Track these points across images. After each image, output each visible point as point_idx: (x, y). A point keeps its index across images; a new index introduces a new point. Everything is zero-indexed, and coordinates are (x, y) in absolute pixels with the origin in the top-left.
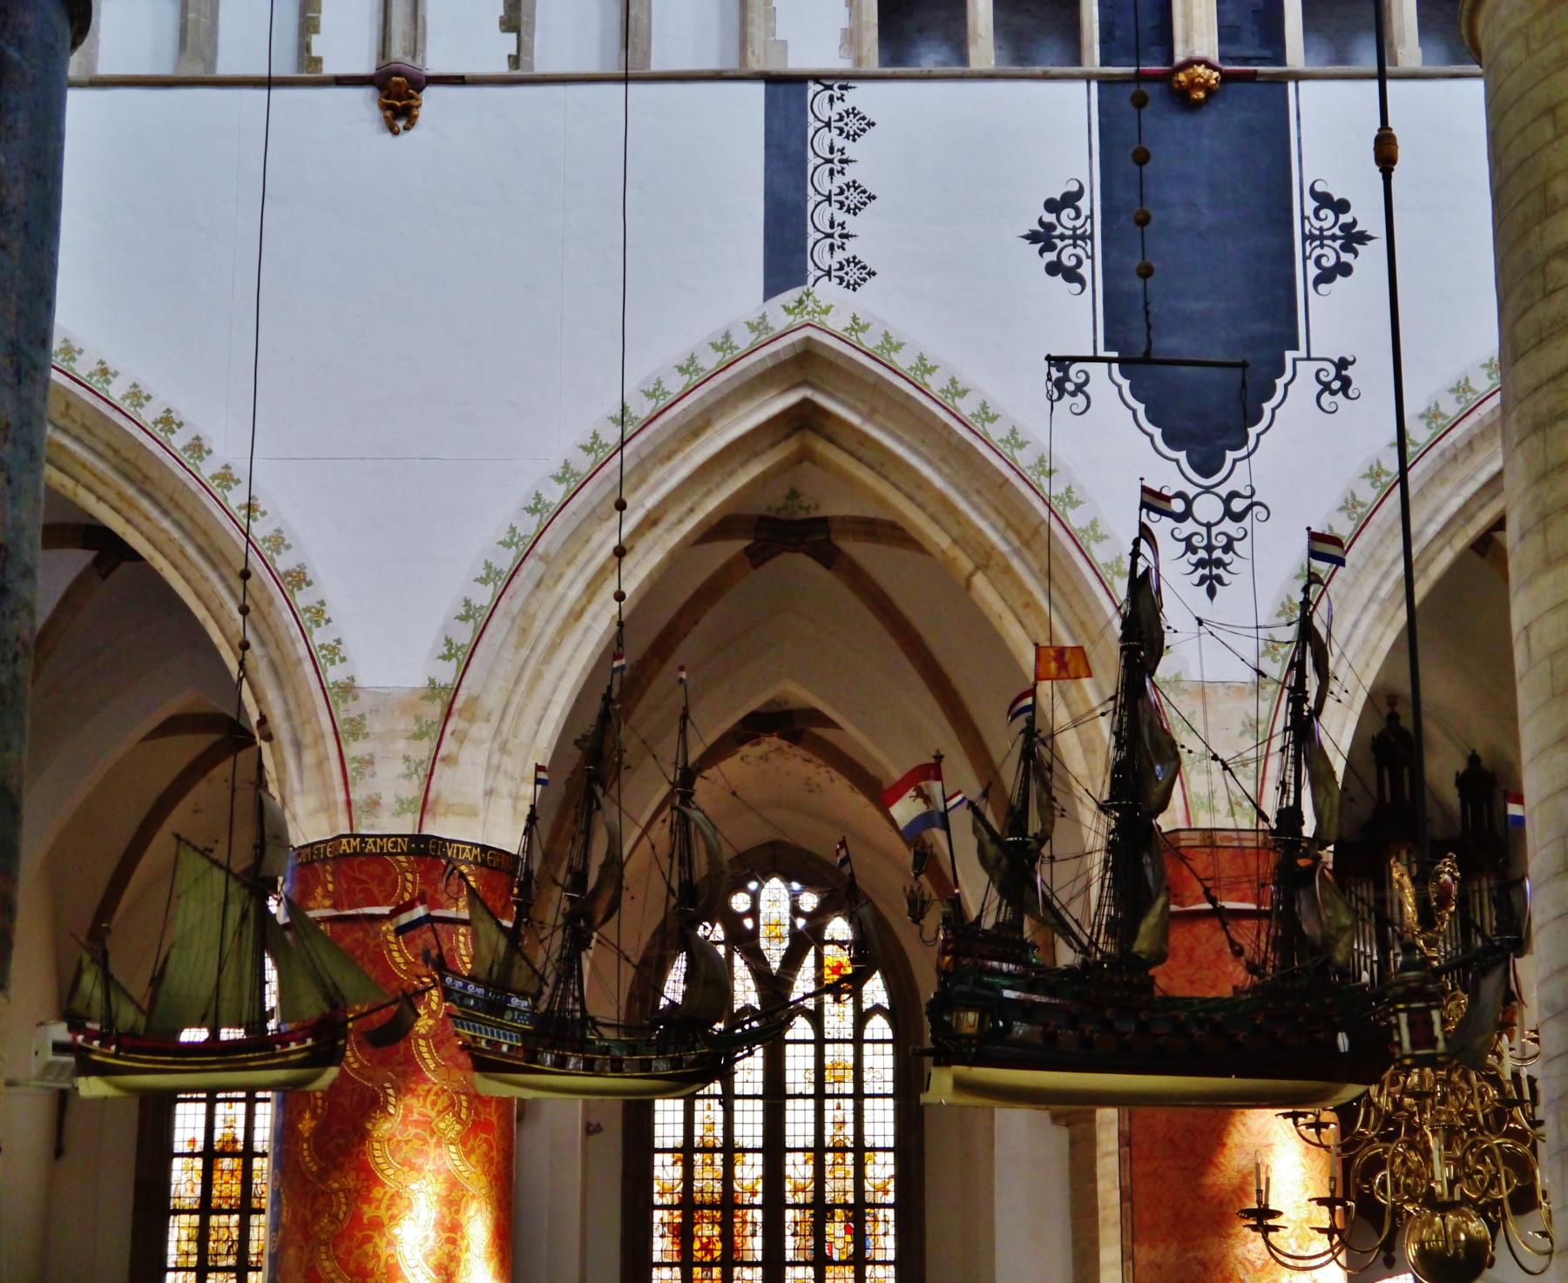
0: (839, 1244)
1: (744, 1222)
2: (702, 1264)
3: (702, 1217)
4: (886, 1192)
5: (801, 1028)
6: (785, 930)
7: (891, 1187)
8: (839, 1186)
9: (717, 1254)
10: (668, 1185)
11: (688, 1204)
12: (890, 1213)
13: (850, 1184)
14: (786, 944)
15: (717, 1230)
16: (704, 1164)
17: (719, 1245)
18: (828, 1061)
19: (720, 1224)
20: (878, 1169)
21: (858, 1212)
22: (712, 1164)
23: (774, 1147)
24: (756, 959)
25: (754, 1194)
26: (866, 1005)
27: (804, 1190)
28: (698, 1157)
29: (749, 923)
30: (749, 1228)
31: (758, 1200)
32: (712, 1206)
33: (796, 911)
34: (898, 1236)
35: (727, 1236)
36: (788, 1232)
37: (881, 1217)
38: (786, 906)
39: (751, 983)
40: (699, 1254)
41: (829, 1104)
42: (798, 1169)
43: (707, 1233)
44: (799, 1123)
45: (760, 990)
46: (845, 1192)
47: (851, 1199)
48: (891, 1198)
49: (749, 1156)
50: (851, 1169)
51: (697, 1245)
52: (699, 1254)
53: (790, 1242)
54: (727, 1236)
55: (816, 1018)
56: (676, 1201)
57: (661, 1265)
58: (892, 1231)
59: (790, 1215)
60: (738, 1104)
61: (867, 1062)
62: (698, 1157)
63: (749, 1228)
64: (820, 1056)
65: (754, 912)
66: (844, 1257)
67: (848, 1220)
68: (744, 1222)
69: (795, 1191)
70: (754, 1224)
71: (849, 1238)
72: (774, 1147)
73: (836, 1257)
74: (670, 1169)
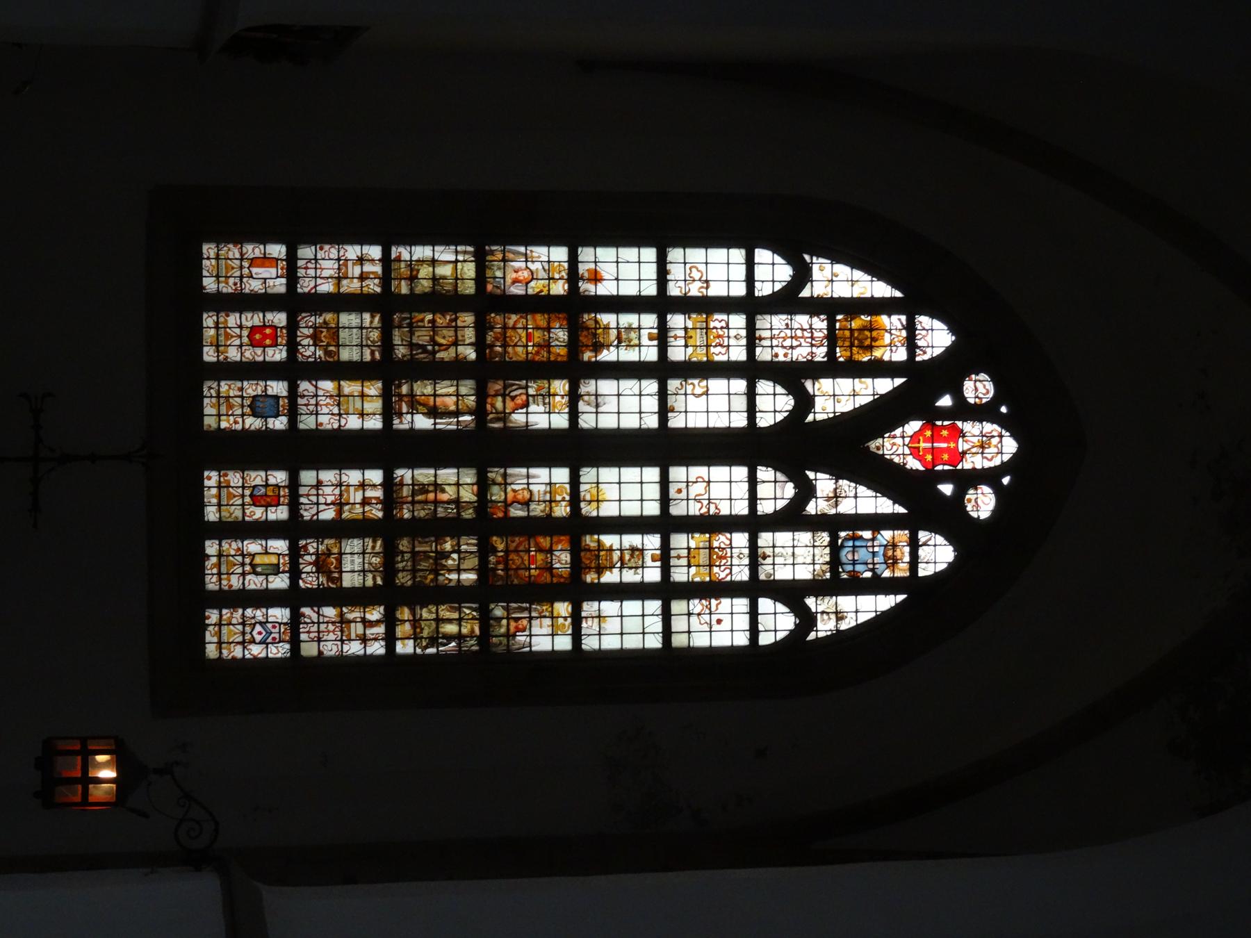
5: (775, 492)
23: (583, 448)
24: (882, 415)
29: (946, 401)
38: (974, 462)
39: (846, 406)
45: (840, 421)
72: (583, 448)
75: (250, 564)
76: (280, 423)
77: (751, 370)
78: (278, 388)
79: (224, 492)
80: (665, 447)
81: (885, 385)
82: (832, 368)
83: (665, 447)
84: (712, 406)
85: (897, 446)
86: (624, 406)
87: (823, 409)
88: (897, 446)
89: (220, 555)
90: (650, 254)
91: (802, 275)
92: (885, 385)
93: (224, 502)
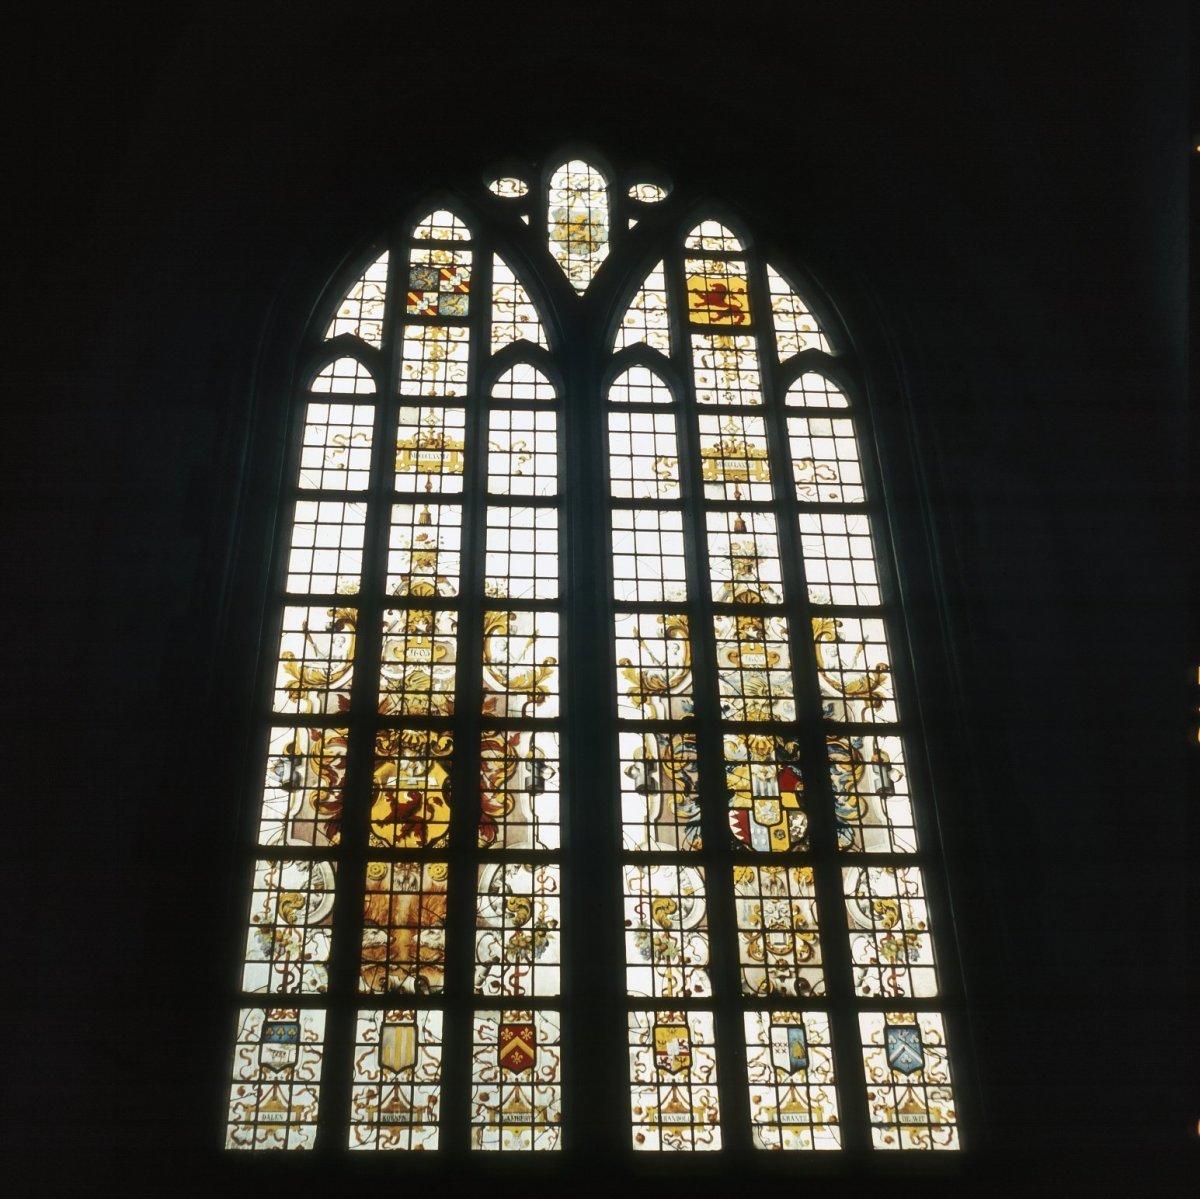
0: (766, 811)
1: (511, 761)
2: (392, 855)
3: (399, 745)
4: (877, 701)
6: (603, 233)
7: (886, 688)
8: (755, 672)
9: (435, 831)
10: (315, 671)
11: (364, 719)
12: (893, 747)
13: (782, 682)
14: (604, 252)
15: (438, 777)
16: (408, 632)
17: (443, 812)
18: (707, 444)
19: (445, 762)
20: (848, 653)
21: (811, 745)
22: (432, 630)
23: (587, 603)
24: (543, 280)
25: (537, 696)
26: (786, 351)
27: (665, 692)
28: (394, 619)
30: (524, 773)
31: (550, 708)
32: (427, 722)
33: (621, 206)
34: (917, 795)
35: (465, 791)
36: (626, 783)
37: (868, 753)
40: (388, 832)
41: (714, 520)
42: (645, 649)
43: (409, 780)
44: (646, 558)
46: (772, 700)
47: (786, 711)
48: (889, 713)
49: (523, 621)
50: (784, 651)
51: (381, 809)
52: (388, 832)
53: (633, 807)
54: (465, 791)
55: (676, 369)
56: (334, 706)
57: (279, 855)
58: (902, 786)
59: (629, 745)
60: (495, 515)
61: (798, 449)
62: (394, 619)
63: (524, 773)
64: (688, 437)
65: (536, 202)
66: (782, 846)
67: (783, 758)
68: (511, 761)
69: (644, 694)
70: (539, 764)
71: (790, 800)
72: (587, 603)
73: (760, 841)
74: (322, 642)
75: (791, 1074)
76: (549, 1024)
77: (478, 404)
78: (485, 1025)
79: (668, 1118)
80: (585, 503)
81: (502, 272)
82: (479, 320)
83: (585, 503)
84: (527, 448)
85: (582, 271)
86: (526, 554)
87: (534, 333)
88: (582, 271)
89: (778, 1125)
90: (304, 510)
91: (351, 346)
92: (502, 272)
93: (687, 1118)
